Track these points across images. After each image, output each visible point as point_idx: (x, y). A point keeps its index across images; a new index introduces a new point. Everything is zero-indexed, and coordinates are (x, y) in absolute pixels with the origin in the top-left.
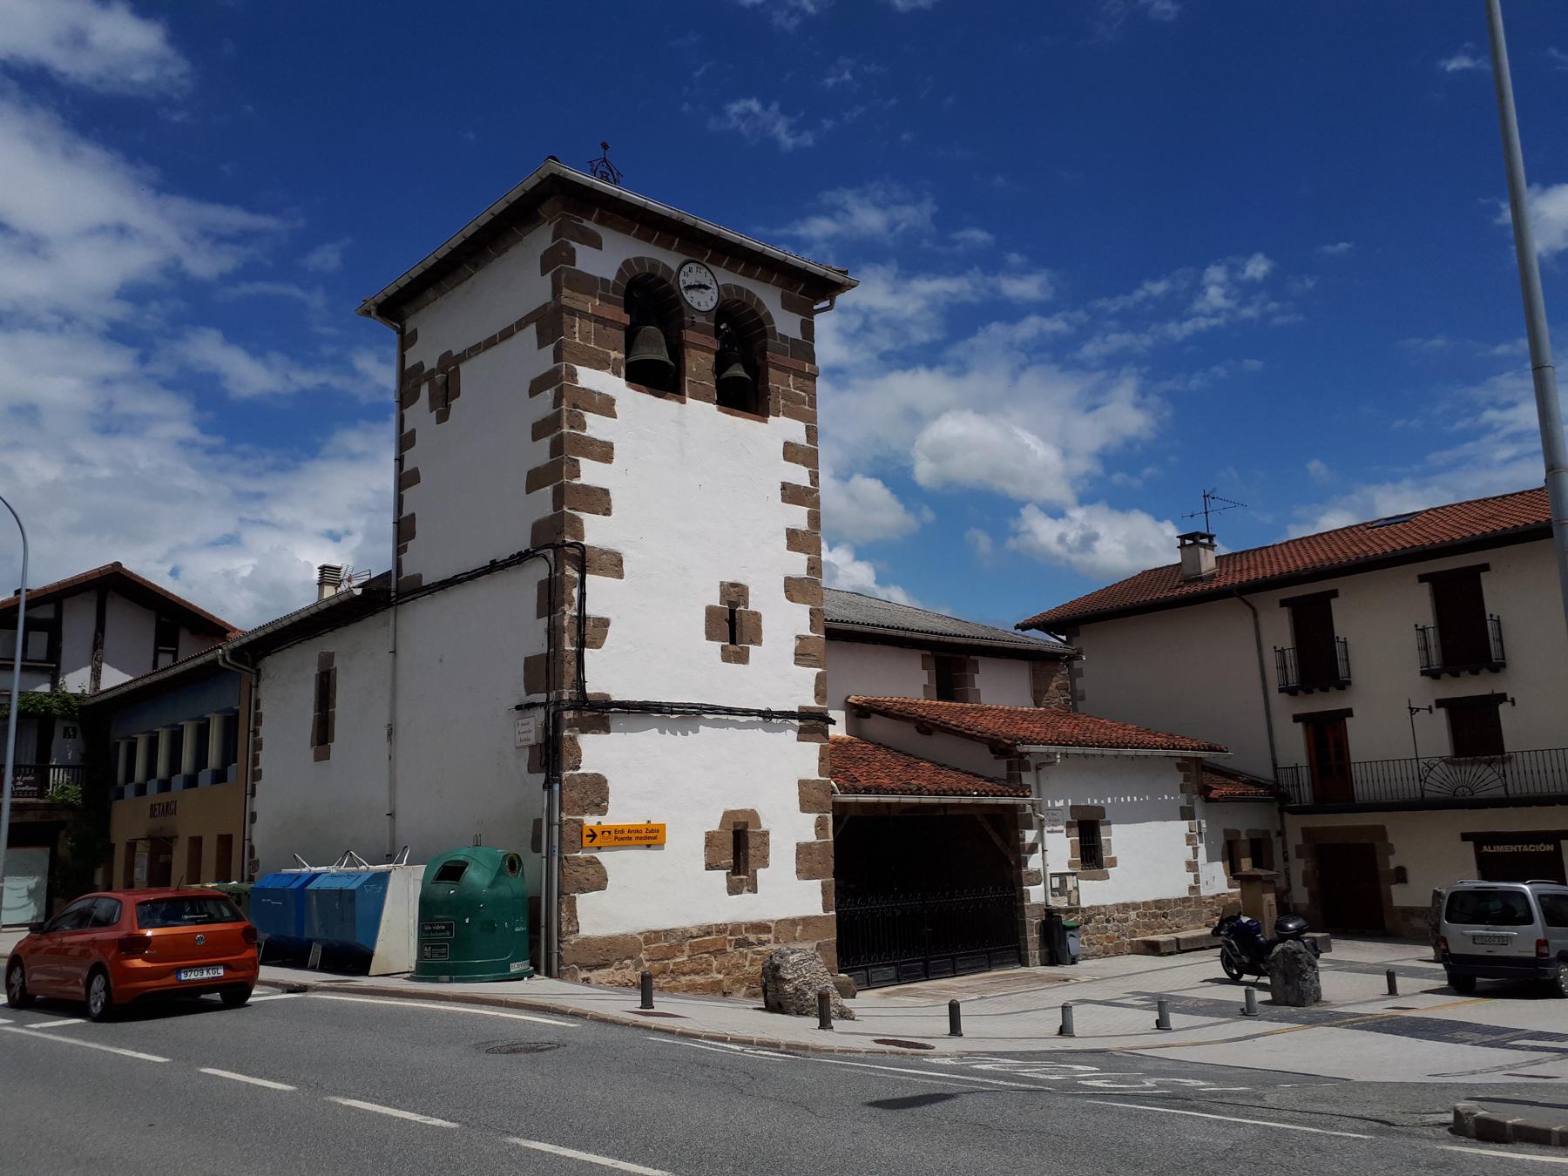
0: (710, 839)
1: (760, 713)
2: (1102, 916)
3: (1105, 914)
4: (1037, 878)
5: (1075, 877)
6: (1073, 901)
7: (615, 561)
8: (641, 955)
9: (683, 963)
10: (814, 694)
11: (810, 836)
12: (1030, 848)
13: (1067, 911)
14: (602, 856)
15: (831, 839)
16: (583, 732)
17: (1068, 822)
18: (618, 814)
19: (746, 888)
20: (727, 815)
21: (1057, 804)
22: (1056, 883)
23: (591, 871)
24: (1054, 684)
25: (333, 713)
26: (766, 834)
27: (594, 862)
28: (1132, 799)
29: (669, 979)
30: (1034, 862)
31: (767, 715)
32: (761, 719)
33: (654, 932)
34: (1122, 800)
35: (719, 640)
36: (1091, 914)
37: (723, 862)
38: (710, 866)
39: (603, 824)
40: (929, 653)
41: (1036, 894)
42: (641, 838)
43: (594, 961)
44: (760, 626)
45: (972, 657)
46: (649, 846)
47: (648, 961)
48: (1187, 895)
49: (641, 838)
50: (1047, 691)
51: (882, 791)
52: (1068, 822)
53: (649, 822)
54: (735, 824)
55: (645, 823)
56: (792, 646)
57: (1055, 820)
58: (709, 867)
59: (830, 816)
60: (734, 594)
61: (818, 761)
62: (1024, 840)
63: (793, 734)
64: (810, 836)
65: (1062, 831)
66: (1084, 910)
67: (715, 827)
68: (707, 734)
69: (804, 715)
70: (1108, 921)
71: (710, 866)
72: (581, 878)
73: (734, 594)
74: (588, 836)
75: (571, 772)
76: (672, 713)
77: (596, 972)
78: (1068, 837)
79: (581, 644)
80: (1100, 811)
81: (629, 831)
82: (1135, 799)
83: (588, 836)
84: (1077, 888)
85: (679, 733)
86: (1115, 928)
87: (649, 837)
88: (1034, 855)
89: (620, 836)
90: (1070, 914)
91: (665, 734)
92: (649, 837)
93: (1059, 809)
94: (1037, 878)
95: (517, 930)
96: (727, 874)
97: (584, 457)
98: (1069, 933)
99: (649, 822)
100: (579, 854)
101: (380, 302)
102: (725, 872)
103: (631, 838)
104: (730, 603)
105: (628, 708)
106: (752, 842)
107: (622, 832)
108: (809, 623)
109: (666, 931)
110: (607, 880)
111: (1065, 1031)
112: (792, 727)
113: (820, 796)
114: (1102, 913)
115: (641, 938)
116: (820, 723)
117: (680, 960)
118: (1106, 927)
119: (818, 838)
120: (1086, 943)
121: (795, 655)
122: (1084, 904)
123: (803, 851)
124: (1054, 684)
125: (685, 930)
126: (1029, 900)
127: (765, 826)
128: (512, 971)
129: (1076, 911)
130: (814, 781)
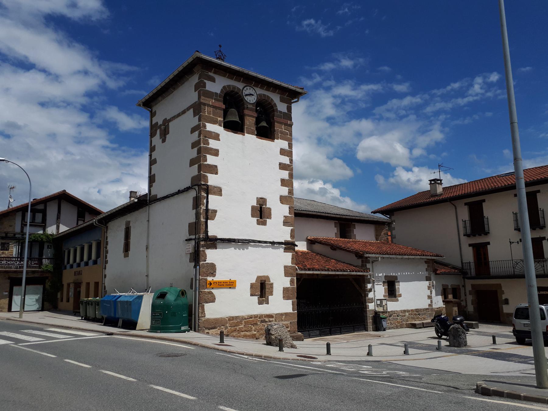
0: (252, 286)
1: (270, 243)
2: (396, 314)
3: (397, 314)
4: (372, 301)
5: (386, 301)
6: (385, 309)
7: (219, 190)
8: (227, 325)
9: (242, 328)
10: (290, 236)
11: (288, 285)
12: (369, 290)
13: (383, 312)
14: (214, 291)
15: (296, 286)
16: (207, 249)
17: (383, 281)
18: (220, 277)
19: (265, 303)
20: (258, 277)
21: (380, 275)
22: (379, 302)
23: (210, 296)
24: (383, 233)
25: (130, 241)
26: (272, 284)
27: (211, 293)
28: (405, 273)
29: (237, 333)
30: (371, 295)
31: (273, 243)
32: (271, 245)
33: (232, 317)
34: (404, 274)
35: (256, 217)
36: (392, 313)
37: (256, 293)
38: (252, 295)
39: (214, 280)
40: (337, 222)
41: (371, 306)
42: (227, 285)
43: (210, 327)
44: (271, 212)
45: (353, 223)
46: (230, 288)
47: (229, 327)
48: (428, 307)
49: (227, 285)
50: (380, 235)
51: (315, 270)
52: (383, 281)
53: (230, 279)
54: (261, 281)
55: (229, 280)
56: (282, 219)
57: (379, 281)
58: (252, 295)
59: (295, 278)
60: (262, 202)
61: (291, 259)
62: (367, 287)
63: (282, 250)
64: (288, 285)
65: (381, 284)
66: (389, 312)
67: (254, 281)
68: (251, 250)
69: (286, 243)
70: (398, 316)
71: (252, 295)
72: (206, 299)
73: (262, 202)
74: (209, 284)
75: (203, 262)
76: (239, 242)
77: (211, 330)
78: (383, 286)
79: (207, 219)
80: (396, 277)
81: (223, 283)
82: (409, 273)
83: (209, 284)
84: (386, 304)
85: (241, 249)
86: (400, 319)
87: (230, 285)
88: (371, 293)
89: (220, 284)
90: (384, 313)
92: (230, 285)
93: (380, 277)
94: (372, 301)
95: (184, 315)
96: (258, 298)
97: (208, 154)
98: (383, 320)
99: (230, 279)
100: (206, 290)
101: (144, 101)
102: (257, 297)
103: (224, 285)
104: (260, 204)
105: (223, 240)
106: (267, 287)
107: (221, 283)
108: (289, 211)
109: (236, 317)
110: (215, 299)
111: (369, 354)
112: (282, 247)
113: (291, 271)
114: (396, 313)
115: (227, 319)
116: (292, 246)
117: (241, 327)
118: (397, 318)
119: (291, 286)
120: (389, 323)
121: (283, 222)
122: (389, 310)
123: (285, 290)
124: (383, 233)
125: (243, 317)
126: (369, 308)
127: (272, 281)
128: (182, 329)
129: (386, 312)
130: (290, 266)
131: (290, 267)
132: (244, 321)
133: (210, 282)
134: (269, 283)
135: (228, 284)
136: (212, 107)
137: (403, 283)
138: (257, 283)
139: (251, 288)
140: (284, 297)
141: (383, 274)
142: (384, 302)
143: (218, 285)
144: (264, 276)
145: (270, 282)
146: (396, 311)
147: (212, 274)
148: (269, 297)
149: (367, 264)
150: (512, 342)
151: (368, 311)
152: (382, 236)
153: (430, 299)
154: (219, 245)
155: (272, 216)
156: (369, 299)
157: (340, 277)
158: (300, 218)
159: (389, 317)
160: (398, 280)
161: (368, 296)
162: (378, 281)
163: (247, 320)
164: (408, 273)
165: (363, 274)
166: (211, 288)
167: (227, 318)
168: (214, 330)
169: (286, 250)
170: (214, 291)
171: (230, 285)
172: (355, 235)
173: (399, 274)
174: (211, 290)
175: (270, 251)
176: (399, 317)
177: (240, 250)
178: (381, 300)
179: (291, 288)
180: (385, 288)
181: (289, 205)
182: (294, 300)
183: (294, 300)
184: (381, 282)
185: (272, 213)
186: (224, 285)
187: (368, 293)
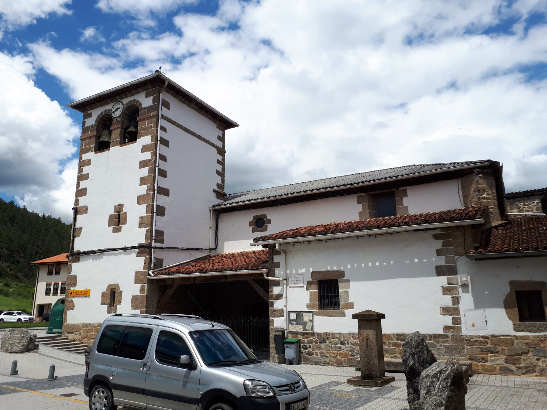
0: (103, 294)
1: (122, 249)
2: (337, 340)
3: (340, 339)
4: (280, 313)
5: (311, 314)
6: (308, 327)
7: (86, 209)
8: (81, 331)
9: (92, 335)
10: (144, 238)
11: (137, 293)
12: (276, 297)
13: (304, 334)
14: (74, 300)
15: (146, 293)
16: (73, 263)
17: (308, 282)
18: (80, 287)
19: (113, 312)
20: (109, 286)
21: (300, 271)
22: (293, 316)
23: (71, 304)
24: (472, 189)
26: (122, 292)
27: (72, 301)
28: (366, 265)
29: (88, 340)
30: (278, 305)
31: (125, 249)
32: (123, 251)
33: (85, 324)
34: (363, 265)
35: (112, 226)
36: (323, 338)
37: (106, 302)
38: (102, 304)
39: (87, 289)
40: (363, 194)
41: (278, 323)
42: (83, 294)
43: (69, 331)
44: (127, 217)
45: (401, 189)
46: (86, 297)
47: (83, 333)
48: (441, 332)
49: (83, 294)
50: (469, 195)
51: (213, 271)
52: (308, 282)
53: (86, 289)
54: (111, 289)
55: (85, 289)
56: (138, 220)
57: (297, 281)
58: (102, 304)
59: (146, 285)
60: (119, 208)
61: (144, 264)
62: (272, 292)
63: (134, 255)
64: (137, 293)
65: (303, 287)
66: (319, 334)
67: (105, 290)
68: (106, 259)
69: (140, 247)
70: (343, 343)
71: (102, 304)
72: (68, 306)
73: (119, 208)
74: (70, 293)
75: (69, 275)
76: (96, 253)
77: (70, 334)
78: (307, 290)
79: (74, 237)
80: (341, 274)
81: (80, 292)
82: (377, 264)
83: (70, 293)
84: (312, 321)
85: (97, 260)
86: (349, 349)
87: (85, 294)
88: (279, 301)
89: (78, 293)
90: (306, 336)
91: (96, 260)
92: (85, 294)
93: (302, 274)
94: (280, 313)
95: (57, 320)
96: (107, 306)
97: (81, 181)
98: (286, 346)
99: (86, 289)
100: (68, 299)
102: (106, 306)
103: (80, 294)
104: (117, 212)
105: (88, 253)
106: (117, 295)
107: (78, 292)
108: (146, 210)
109: (88, 324)
110: (74, 307)
111: (15, 372)
112: (135, 252)
113: (142, 277)
114: (337, 338)
115: (81, 325)
116: (146, 249)
117: (91, 334)
118: (340, 347)
119: (140, 294)
120: (319, 354)
121: (139, 224)
122: (317, 330)
123: (134, 298)
124: (472, 189)
125: (93, 324)
126: (273, 325)
127: (121, 290)
128: (53, 331)
129: (313, 334)
130: (141, 272)
131: (141, 273)
132: (94, 329)
133: (71, 292)
134: (118, 291)
135: (84, 293)
136: (88, 138)
137: (359, 282)
138: (107, 291)
139: (102, 296)
140: (132, 306)
141: (308, 270)
142: (306, 317)
143: (77, 294)
144: (114, 285)
145: (119, 290)
146: (338, 334)
147: (74, 284)
148: (117, 305)
149: (273, 256)
150: (65, 394)
151: (272, 329)
152: (471, 196)
153: (450, 315)
154: (82, 258)
155: (127, 221)
156: (275, 311)
157: (228, 280)
158: (295, 204)
159: (320, 343)
160: (345, 278)
161: (273, 305)
162: (295, 282)
163: (96, 328)
164: (374, 264)
165: (247, 272)
166: (72, 297)
167: (81, 324)
168: (72, 334)
169: (139, 255)
170: (74, 300)
171: (85, 294)
172: (407, 206)
173: (349, 266)
174: (72, 299)
175: (122, 257)
176: (346, 345)
177: (96, 260)
178: (300, 314)
179: (141, 296)
180: (310, 292)
181: (146, 203)
182: (142, 310)
183: (142, 310)
184: (301, 283)
185: (127, 217)
186: (80, 294)
187: (274, 301)
